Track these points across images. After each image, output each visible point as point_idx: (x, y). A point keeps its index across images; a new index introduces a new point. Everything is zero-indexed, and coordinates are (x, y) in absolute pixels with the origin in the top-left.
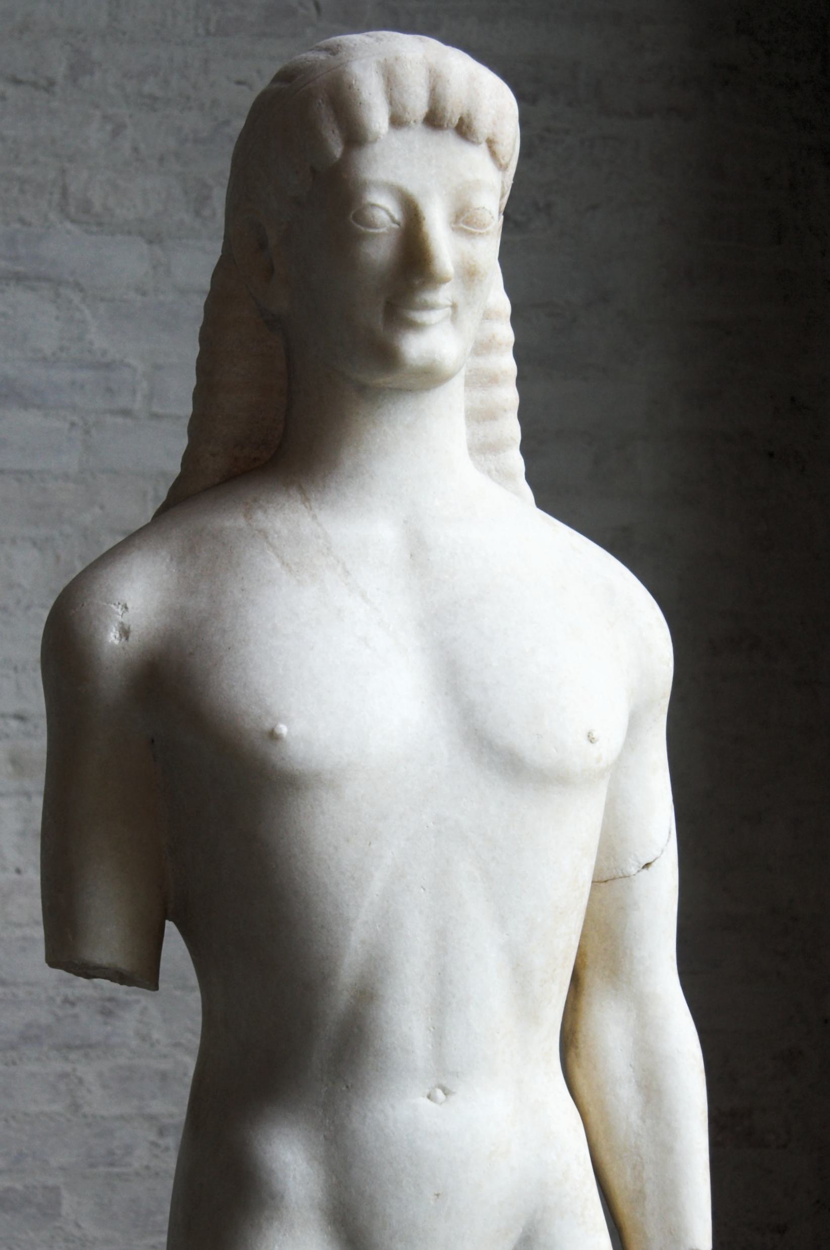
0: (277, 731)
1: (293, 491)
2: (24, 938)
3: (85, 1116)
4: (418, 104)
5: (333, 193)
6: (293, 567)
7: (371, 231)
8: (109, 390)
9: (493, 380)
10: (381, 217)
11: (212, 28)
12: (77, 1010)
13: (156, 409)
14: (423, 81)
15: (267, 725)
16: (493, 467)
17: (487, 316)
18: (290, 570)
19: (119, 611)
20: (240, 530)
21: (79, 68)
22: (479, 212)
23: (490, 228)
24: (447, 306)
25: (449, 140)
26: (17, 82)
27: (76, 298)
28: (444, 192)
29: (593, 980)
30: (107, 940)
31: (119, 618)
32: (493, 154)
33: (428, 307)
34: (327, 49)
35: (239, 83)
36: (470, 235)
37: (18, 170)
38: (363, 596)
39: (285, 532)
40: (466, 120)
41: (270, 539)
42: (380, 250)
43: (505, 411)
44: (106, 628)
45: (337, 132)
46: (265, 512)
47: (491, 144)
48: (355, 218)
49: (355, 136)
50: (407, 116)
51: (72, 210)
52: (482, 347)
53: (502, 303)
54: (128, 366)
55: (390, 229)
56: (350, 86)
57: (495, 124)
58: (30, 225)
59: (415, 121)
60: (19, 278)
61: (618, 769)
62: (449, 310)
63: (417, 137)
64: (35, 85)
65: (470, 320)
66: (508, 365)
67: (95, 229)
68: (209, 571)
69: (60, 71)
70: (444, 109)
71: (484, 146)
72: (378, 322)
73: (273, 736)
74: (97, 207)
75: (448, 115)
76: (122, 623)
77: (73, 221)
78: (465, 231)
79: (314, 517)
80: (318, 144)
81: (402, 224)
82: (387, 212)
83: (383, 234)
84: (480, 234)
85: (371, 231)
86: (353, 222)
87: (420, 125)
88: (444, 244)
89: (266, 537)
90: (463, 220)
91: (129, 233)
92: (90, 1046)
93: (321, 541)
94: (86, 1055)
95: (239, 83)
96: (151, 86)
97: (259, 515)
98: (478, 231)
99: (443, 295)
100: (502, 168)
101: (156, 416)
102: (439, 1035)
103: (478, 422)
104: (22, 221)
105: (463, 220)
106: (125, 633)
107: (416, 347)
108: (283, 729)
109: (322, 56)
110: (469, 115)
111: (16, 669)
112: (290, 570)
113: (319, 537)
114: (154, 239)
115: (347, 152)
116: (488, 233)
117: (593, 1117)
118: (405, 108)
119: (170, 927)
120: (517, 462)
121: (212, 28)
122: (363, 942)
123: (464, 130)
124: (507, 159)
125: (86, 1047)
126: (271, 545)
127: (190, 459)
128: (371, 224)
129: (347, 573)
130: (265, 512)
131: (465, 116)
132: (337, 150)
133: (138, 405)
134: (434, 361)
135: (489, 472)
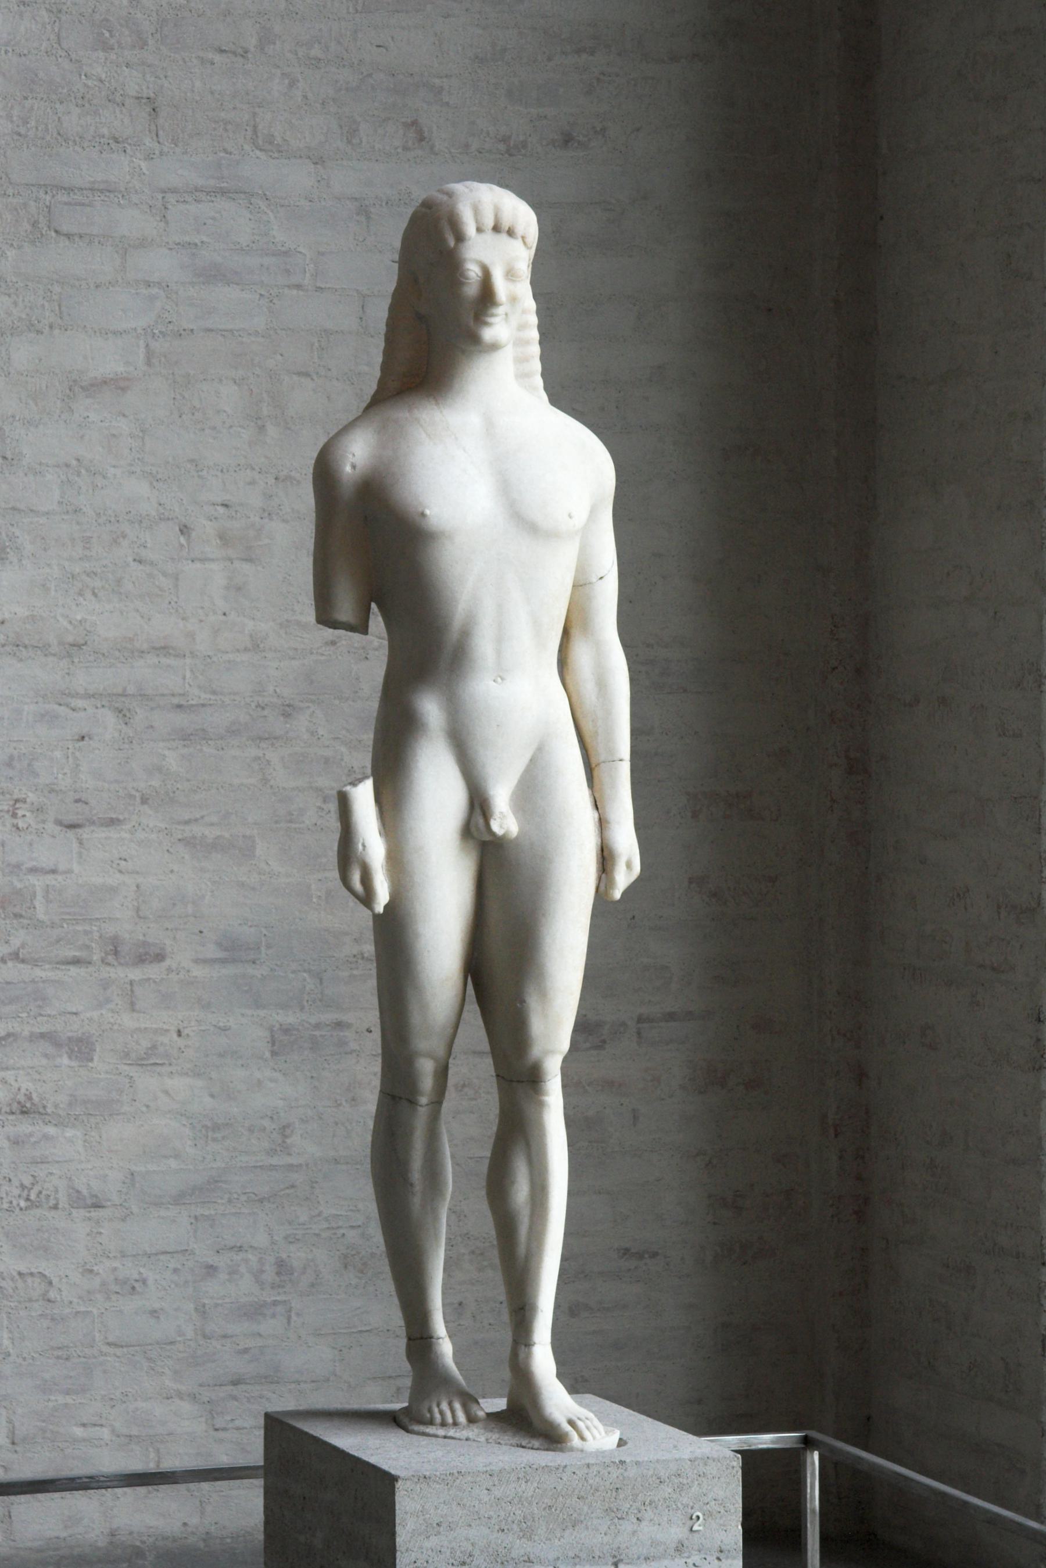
2: (229, 662)
3: (271, 787)
4: (489, 222)
8: (288, 271)
9: (527, 342)
11: (359, 9)
12: (266, 713)
13: (319, 284)
15: (420, 510)
17: (524, 312)
21: (266, 39)
25: (504, 237)
26: (222, 51)
27: (263, 205)
29: (575, 632)
30: (345, 611)
32: (525, 243)
33: (493, 315)
36: (514, 281)
37: (223, 114)
42: (471, 290)
47: (523, 238)
49: (460, 237)
51: (260, 142)
52: (522, 327)
53: (531, 304)
54: (300, 252)
58: (231, 153)
60: (223, 192)
61: (586, 533)
63: (489, 236)
64: (234, 53)
66: (535, 335)
67: (276, 155)
68: (392, 438)
69: (252, 42)
72: (472, 323)
73: (423, 515)
74: (278, 140)
77: (261, 150)
80: (443, 240)
88: (501, 286)
90: (511, 274)
92: (275, 738)
94: (273, 745)
96: (316, 51)
97: (416, 411)
99: (500, 311)
100: (529, 248)
102: (499, 653)
104: (225, 151)
105: (511, 274)
106: (354, 467)
107: (488, 334)
108: (428, 512)
109: (445, 198)
111: (222, 471)
114: (319, 161)
117: (574, 700)
119: (373, 605)
120: (539, 382)
123: (511, 233)
125: (271, 739)
126: (421, 426)
127: (382, 382)
128: (467, 279)
129: (456, 439)
132: (452, 242)
133: (307, 281)
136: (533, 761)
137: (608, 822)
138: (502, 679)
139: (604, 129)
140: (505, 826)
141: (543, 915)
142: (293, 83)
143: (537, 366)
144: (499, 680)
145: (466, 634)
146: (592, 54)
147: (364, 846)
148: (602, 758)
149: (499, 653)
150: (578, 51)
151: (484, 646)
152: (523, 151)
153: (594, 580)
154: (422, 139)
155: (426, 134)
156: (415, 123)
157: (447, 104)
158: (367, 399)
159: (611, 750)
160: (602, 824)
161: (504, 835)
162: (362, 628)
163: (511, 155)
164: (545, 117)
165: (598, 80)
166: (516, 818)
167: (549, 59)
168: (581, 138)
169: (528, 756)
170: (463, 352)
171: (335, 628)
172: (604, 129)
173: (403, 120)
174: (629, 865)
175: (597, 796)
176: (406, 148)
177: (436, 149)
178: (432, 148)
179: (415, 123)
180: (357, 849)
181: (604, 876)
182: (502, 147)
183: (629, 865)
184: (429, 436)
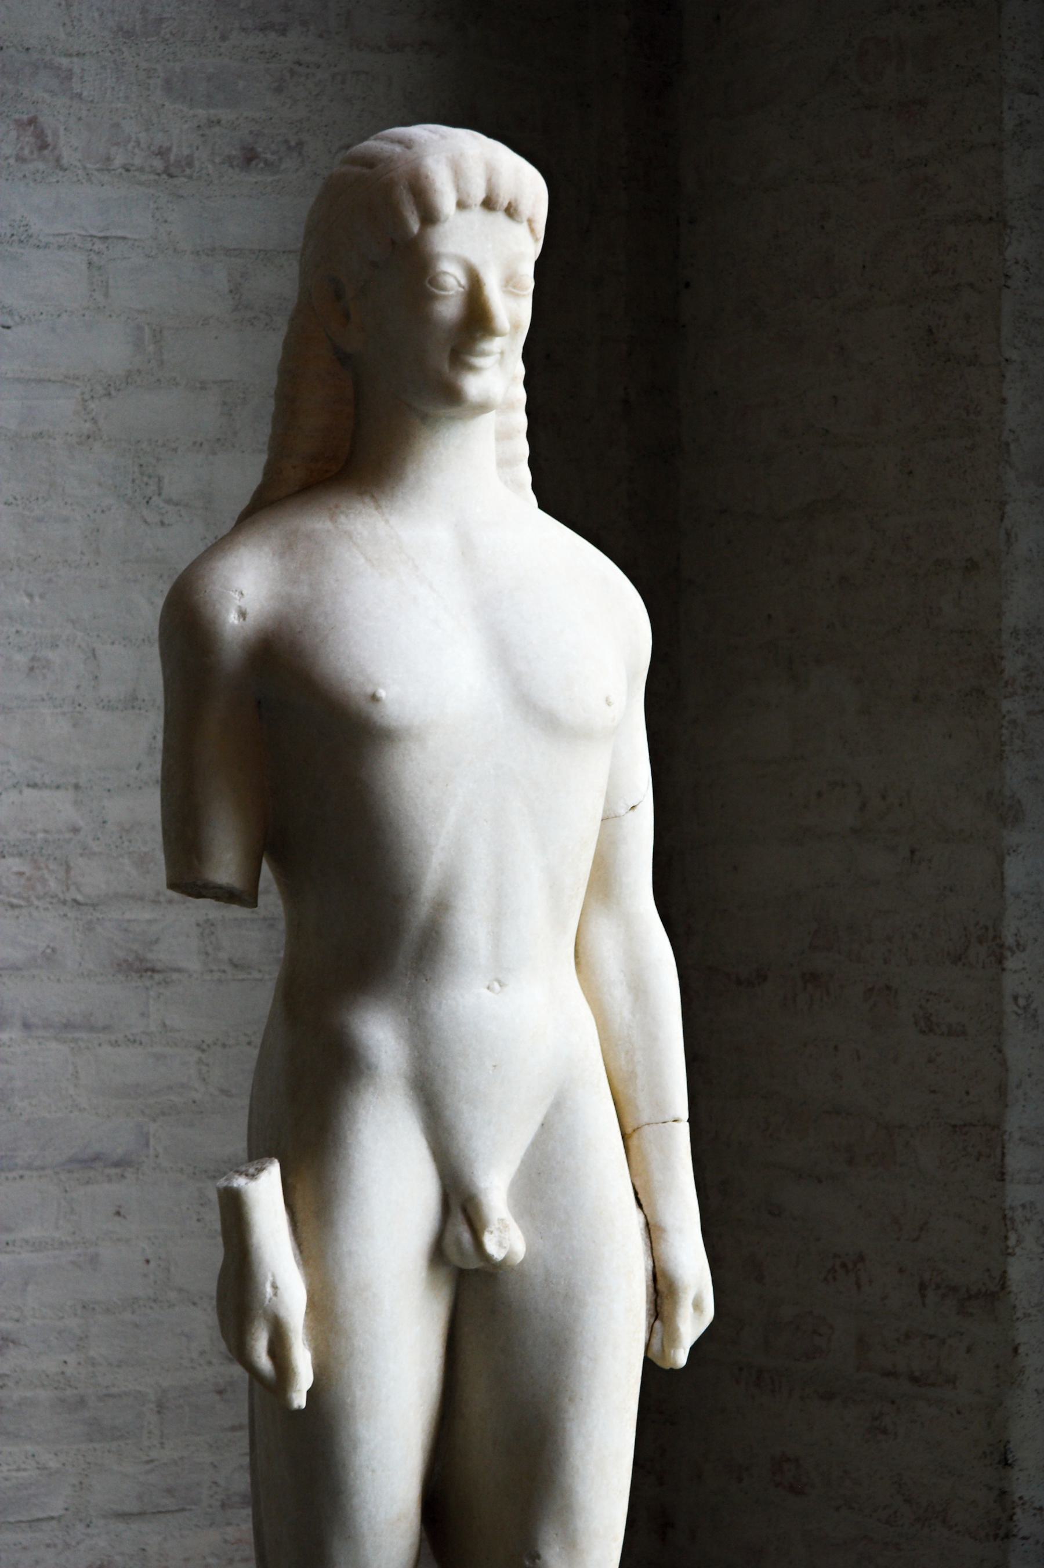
0: (378, 695)
1: (367, 499)
5: (409, 261)
7: (443, 293)
15: (369, 690)
19: (237, 596)
20: (328, 531)
23: (526, 289)
25: (500, 217)
33: (483, 354)
34: (400, 142)
39: (365, 533)
40: (513, 204)
42: (449, 308)
44: (227, 611)
45: (415, 212)
46: (347, 516)
47: (530, 222)
48: (431, 282)
49: (429, 216)
50: (470, 202)
55: (457, 292)
56: (427, 177)
62: (498, 356)
63: (477, 215)
70: (498, 195)
72: (446, 367)
73: (374, 698)
75: (501, 200)
76: (240, 607)
79: (387, 521)
80: (401, 223)
81: (467, 287)
83: (452, 296)
85: (443, 293)
86: (428, 286)
89: (351, 538)
97: (342, 519)
105: (510, 282)
106: (243, 614)
108: (382, 693)
109: (398, 149)
110: (516, 200)
118: (469, 195)
122: (441, 864)
123: (511, 212)
126: (355, 544)
130: (347, 516)
132: (415, 226)
135: (506, 483)
136: (545, 1127)
137: (662, 1230)
138: (501, 984)
139: (300, 144)
140: (506, 1244)
141: (571, 1400)
144: (496, 985)
145: (443, 906)
146: (283, 32)
147: (275, 1287)
148: (645, 1118)
149: (497, 940)
150: (263, 29)
151: (472, 929)
152: (188, 171)
153: (622, 811)
154: (43, 146)
155: (50, 139)
156: (32, 121)
157: (79, 96)
159: (660, 1104)
160: (652, 1231)
161: (504, 1260)
162: (244, 896)
163: (171, 176)
164: (219, 122)
165: (292, 73)
166: (521, 1227)
167: (224, 38)
168: (268, 156)
169: (539, 1118)
170: (424, 418)
171: (199, 896)
172: (300, 144)
173: (17, 116)
174: (697, 1306)
175: (637, 1185)
176: (20, 159)
177: (65, 162)
178: (58, 160)
179: (32, 121)
180: (264, 1294)
181: (658, 1324)
182: (158, 164)
183: (697, 1306)
184: (368, 560)
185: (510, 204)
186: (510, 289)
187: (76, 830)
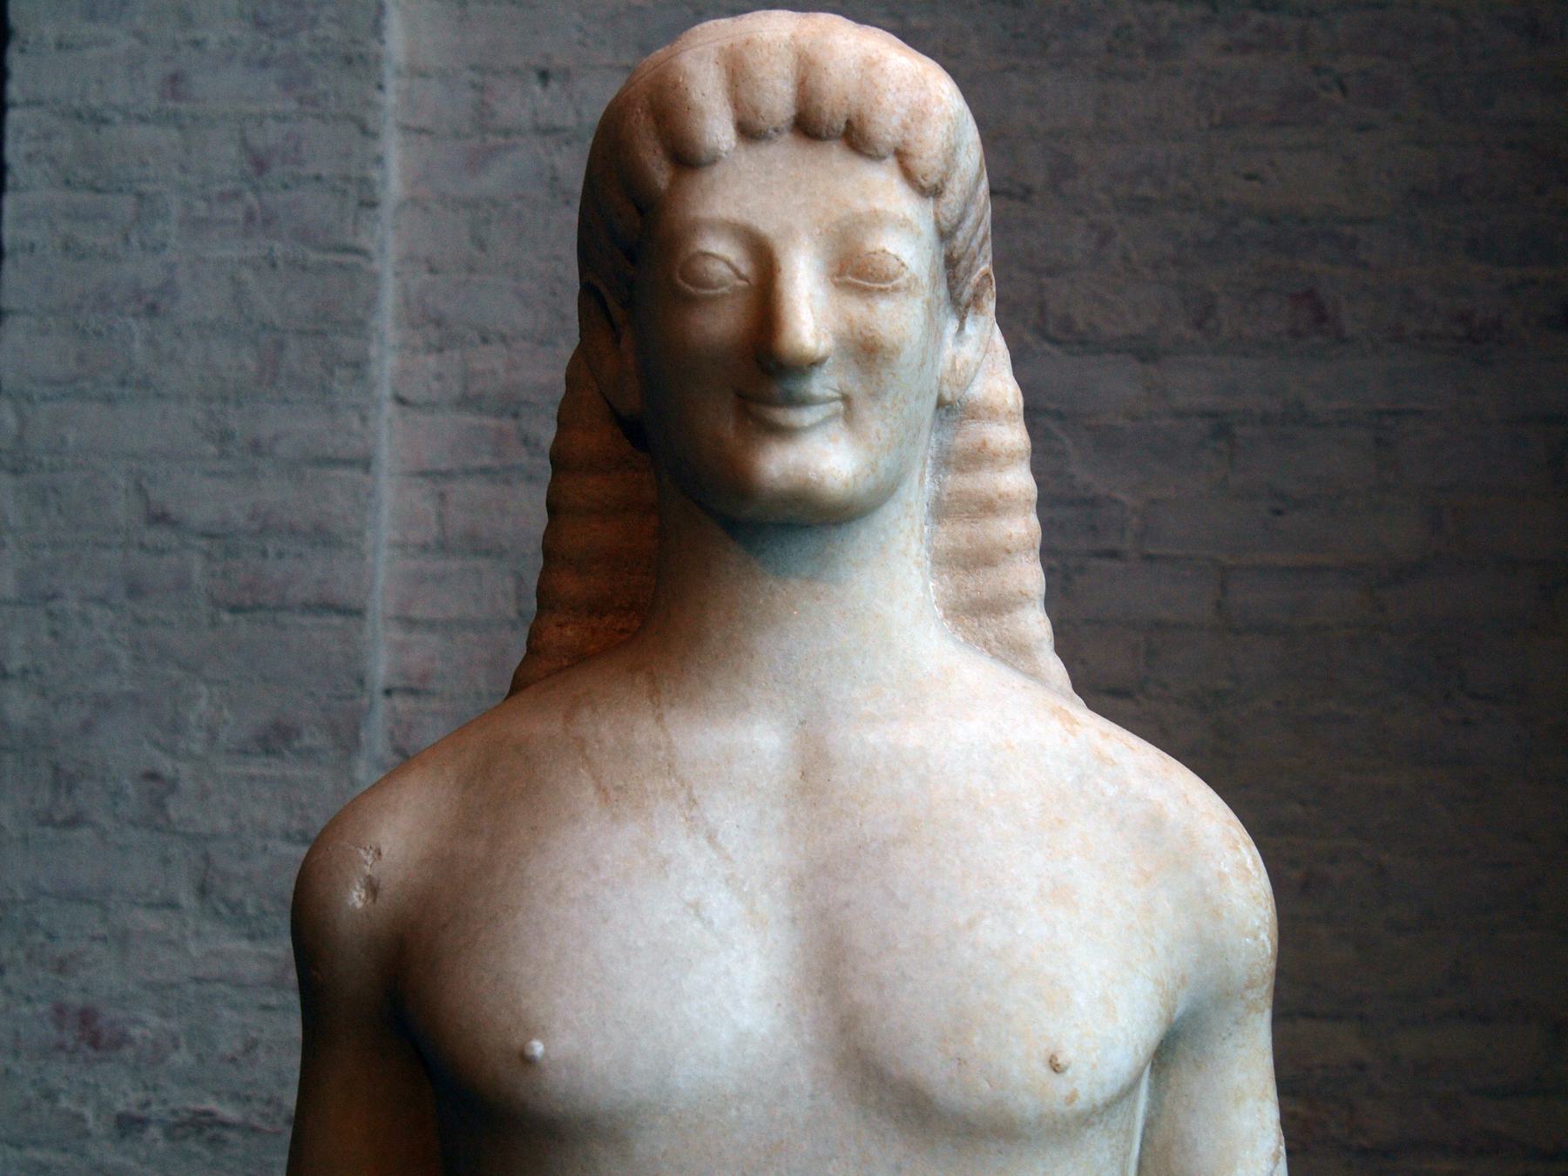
0: (528, 1052)
6: (613, 794)
7: (705, 292)
9: (989, 507)
10: (719, 270)
14: (786, 71)
15: (517, 1041)
16: (991, 636)
18: (607, 799)
19: (369, 859)
22: (877, 258)
24: (833, 400)
25: (835, 155)
28: (818, 231)
31: (367, 868)
32: (908, 175)
33: (804, 402)
35: (1249, 177)
36: (864, 292)
38: (711, 838)
40: (856, 125)
41: (588, 752)
42: (720, 323)
43: (1008, 552)
45: (659, 152)
46: (594, 710)
47: (902, 158)
49: (687, 159)
54: (1115, 501)
56: (676, 85)
57: (905, 127)
59: (776, 130)
62: (840, 406)
63: (783, 154)
65: (877, 423)
68: (502, 796)
69: (1038, 178)
71: (891, 161)
72: (728, 429)
75: (827, 118)
78: (855, 286)
79: (659, 718)
82: (728, 263)
83: (723, 295)
84: (881, 290)
85: (705, 292)
86: (679, 281)
87: (787, 136)
89: (583, 749)
90: (855, 272)
91: (1118, 352)
93: (661, 754)
95: (1249, 177)
98: (889, 285)
99: (821, 384)
101: (1149, 558)
103: (965, 568)
105: (855, 272)
106: (373, 889)
108: (538, 1048)
110: (860, 117)
112: (607, 799)
113: (658, 748)
115: (674, 182)
116: (896, 289)
118: (756, 111)
121: (1217, 119)
123: (856, 138)
124: (934, 179)
126: (588, 760)
128: (707, 284)
129: (692, 802)
130: (594, 710)
131: (854, 118)
132: (661, 174)
134: (808, 481)
135: (986, 643)
142: (1105, 238)
143: (1030, 576)
154: (1321, 317)
156: (1310, 294)
158: (507, 689)
179: (1310, 294)
184: (601, 789)
185: (848, 123)
186: (850, 278)
187: (1361, 1067)
